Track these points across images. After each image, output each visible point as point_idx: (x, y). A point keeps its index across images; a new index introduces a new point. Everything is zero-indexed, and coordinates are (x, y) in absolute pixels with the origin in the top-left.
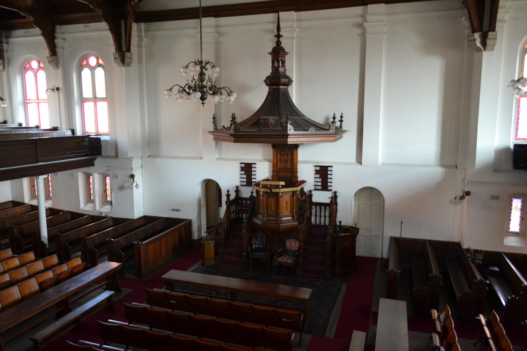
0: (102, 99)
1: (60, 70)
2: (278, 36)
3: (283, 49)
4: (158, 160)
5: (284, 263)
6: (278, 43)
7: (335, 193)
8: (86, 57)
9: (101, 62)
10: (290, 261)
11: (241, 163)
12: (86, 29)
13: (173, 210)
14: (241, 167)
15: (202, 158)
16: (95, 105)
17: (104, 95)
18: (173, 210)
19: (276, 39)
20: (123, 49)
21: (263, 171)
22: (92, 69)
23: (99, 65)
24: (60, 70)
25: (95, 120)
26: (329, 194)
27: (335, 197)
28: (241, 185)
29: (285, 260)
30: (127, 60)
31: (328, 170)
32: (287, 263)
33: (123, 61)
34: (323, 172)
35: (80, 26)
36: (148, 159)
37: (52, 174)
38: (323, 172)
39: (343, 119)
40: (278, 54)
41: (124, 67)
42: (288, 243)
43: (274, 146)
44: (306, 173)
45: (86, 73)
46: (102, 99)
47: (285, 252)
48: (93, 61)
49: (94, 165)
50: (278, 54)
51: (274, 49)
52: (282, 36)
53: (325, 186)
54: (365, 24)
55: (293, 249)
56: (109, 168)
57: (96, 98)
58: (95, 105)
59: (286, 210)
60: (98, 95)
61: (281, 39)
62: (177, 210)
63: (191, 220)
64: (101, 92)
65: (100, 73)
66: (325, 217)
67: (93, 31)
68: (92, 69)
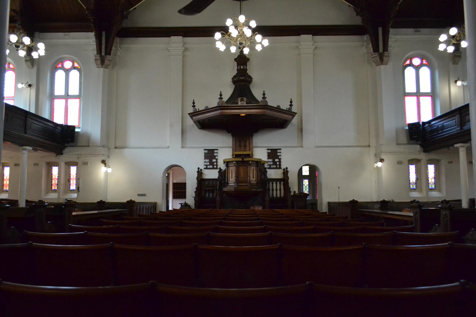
0: (74, 97)
1: (35, 70)
4: (126, 150)
8: (62, 61)
9: (76, 65)
11: (205, 150)
13: (139, 195)
14: (205, 153)
16: (67, 102)
17: (77, 93)
18: (139, 195)
20: (105, 53)
22: (67, 71)
23: (74, 68)
24: (35, 70)
25: (68, 113)
27: (286, 172)
28: (205, 168)
30: (106, 62)
31: (277, 152)
33: (103, 62)
34: (274, 154)
35: (61, 34)
36: (115, 149)
38: (274, 154)
41: (102, 69)
45: (60, 75)
46: (74, 97)
48: (68, 64)
49: (62, 154)
54: (300, 47)
56: (79, 156)
57: (68, 95)
58: (67, 102)
59: (253, 178)
60: (71, 93)
63: (156, 203)
64: (74, 89)
65: (75, 75)
66: (276, 190)
67: (73, 38)
68: (67, 71)
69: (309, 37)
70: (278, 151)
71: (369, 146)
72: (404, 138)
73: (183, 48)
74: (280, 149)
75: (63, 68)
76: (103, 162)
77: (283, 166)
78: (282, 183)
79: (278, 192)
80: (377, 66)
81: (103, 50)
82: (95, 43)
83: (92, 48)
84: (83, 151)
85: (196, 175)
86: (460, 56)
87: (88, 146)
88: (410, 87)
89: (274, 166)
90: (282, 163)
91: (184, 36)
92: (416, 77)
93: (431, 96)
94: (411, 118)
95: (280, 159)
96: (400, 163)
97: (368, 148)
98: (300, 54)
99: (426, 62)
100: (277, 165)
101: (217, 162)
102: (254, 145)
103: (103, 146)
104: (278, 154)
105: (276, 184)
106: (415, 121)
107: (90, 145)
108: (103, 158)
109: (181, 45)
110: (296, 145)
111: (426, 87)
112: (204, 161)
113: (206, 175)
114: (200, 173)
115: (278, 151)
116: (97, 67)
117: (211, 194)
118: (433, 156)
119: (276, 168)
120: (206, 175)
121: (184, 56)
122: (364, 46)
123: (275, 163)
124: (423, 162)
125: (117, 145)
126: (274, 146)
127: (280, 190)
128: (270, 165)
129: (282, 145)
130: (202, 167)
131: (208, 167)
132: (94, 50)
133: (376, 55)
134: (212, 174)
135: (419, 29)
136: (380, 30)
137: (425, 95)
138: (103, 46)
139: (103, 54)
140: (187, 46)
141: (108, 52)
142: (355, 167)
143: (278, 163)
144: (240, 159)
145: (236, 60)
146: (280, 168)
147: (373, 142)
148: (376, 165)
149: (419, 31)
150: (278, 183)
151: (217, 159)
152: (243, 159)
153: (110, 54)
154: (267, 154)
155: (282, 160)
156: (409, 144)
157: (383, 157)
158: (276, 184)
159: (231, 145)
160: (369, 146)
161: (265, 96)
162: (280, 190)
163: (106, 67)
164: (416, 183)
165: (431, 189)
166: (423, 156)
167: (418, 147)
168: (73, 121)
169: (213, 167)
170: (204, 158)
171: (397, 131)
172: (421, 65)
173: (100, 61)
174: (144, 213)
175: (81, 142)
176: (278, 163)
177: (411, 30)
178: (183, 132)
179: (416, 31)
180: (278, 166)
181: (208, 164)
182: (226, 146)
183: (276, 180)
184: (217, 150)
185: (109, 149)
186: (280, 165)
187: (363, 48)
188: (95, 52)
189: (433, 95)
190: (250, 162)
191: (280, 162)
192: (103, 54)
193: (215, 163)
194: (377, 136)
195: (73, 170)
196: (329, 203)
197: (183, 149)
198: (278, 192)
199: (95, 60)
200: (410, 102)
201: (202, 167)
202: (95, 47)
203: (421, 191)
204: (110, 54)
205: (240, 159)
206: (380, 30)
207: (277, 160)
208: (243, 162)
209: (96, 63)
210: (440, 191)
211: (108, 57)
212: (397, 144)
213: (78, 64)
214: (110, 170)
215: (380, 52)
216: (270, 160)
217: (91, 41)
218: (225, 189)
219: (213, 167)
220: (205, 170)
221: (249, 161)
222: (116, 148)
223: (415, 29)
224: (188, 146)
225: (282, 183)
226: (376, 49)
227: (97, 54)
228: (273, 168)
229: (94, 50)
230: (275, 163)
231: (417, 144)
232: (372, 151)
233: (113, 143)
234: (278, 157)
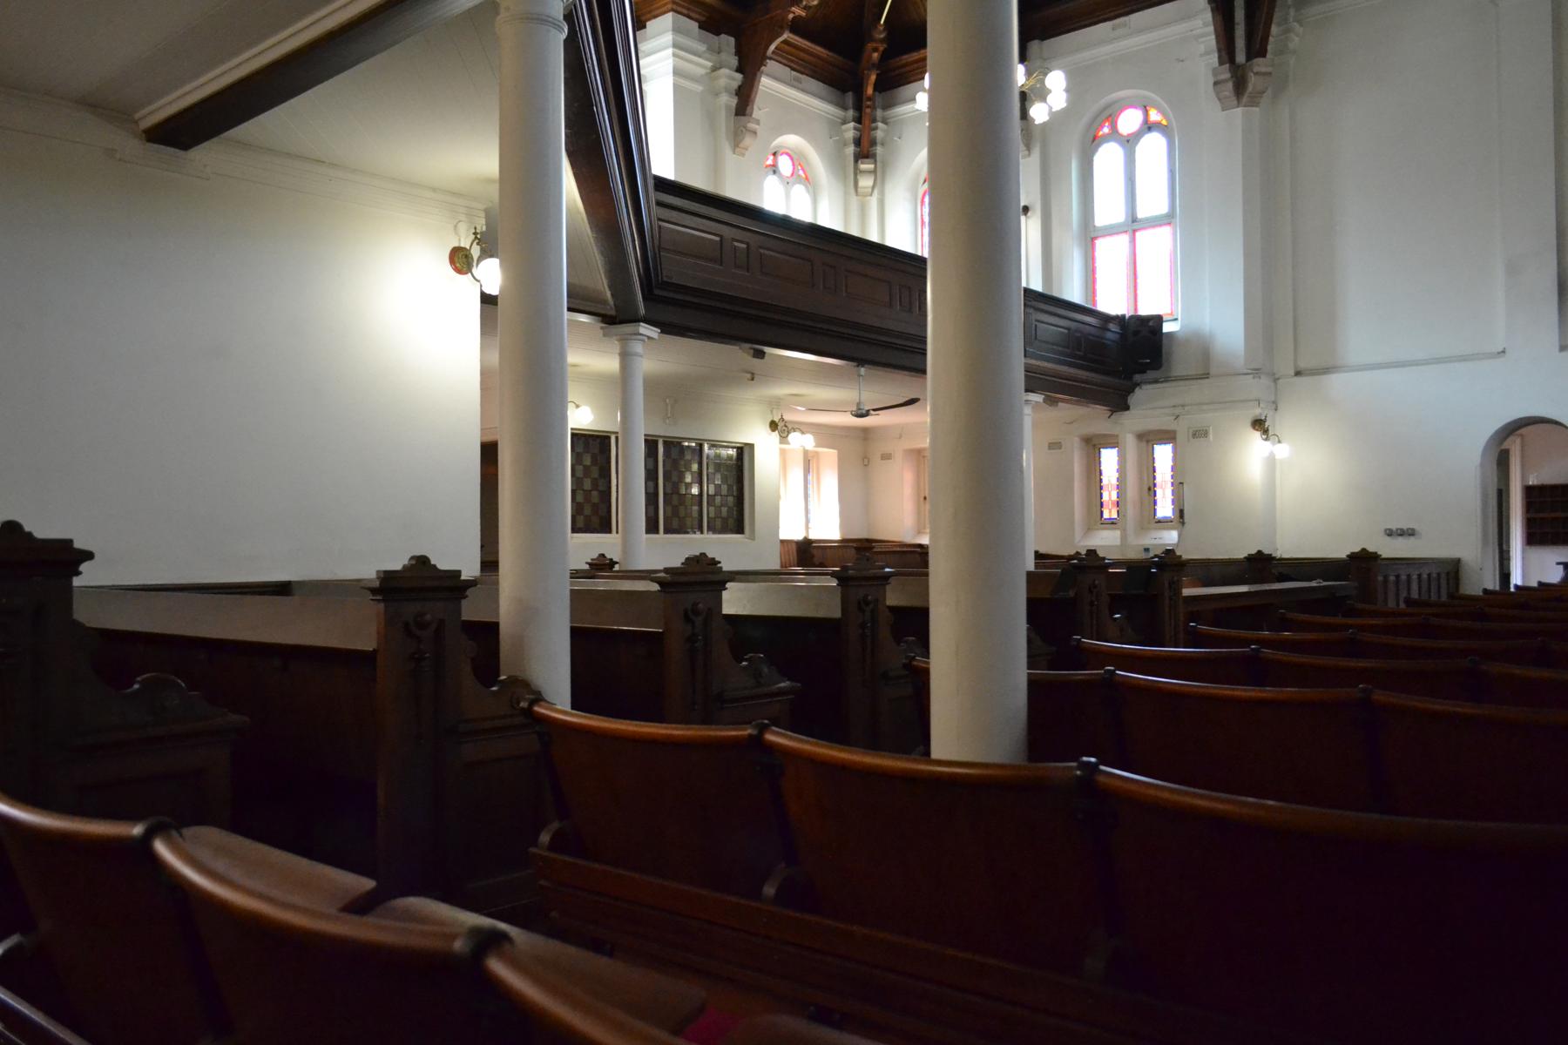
4: (1335, 381)
8: (1110, 115)
9: (1154, 116)
12: (1119, 32)
13: (1390, 533)
16: (1133, 241)
18: (1390, 533)
22: (1130, 142)
23: (1149, 127)
25: (1136, 275)
30: (1253, 82)
33: (1240, 86)
41: (1239, 110)
45: (1108, 158)
48: (1130, 120)
49: (1127, 408)
56: (1177, 411)
57: (1134, 220)
62: (1402, 533)
63: (1459, 561)
64: (1154, 197)
65: (1153, 148)
67: (1140, 31)
75: (1115, 134)
76: (1259, 424)
81: (1240, 43)
82: (1211, 28)
83: (1202, 48)
84: (1192, 393)
87: (1206, 376)
103: (1256, 372)
107: (1213, 371)
108: (1257, 412)
125: (1302, 365)
139: (1241, 57)
141: (1257, 48)
163: (1253, 103)
168: (1154, 299)
173: (1230, 85)
174: (1444, 598)
175: (1180, 363)
185: (1276, 380)
188: (1214, 59)
192: (1241, 57)
195: (1163, 455)
199: (1216, 84)
202: (1211, 41)
209: (1217, 94)
211: (1260, 64)
213: (1161, 111)
214: (1282, 451)
217: (1198, 22)
222: (1298, 373)
227: (1221, 63)
229: (1207, 53)
233: (1290, 356)
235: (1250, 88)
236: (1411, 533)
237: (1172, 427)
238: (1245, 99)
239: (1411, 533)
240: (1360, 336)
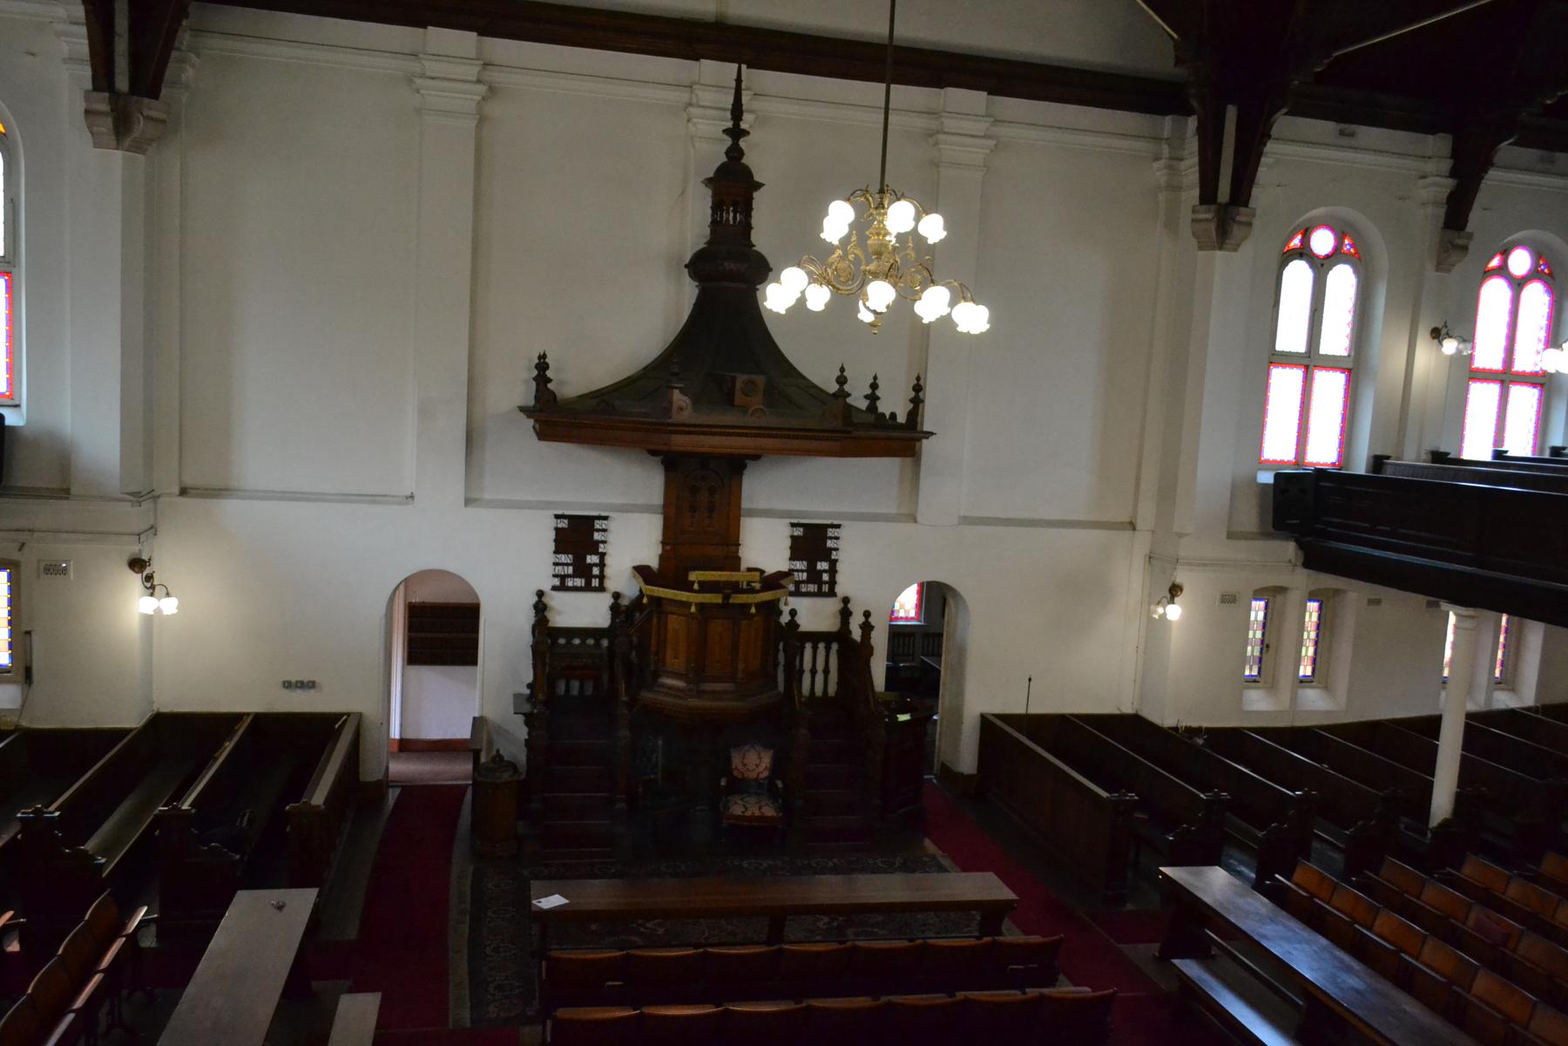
2: (736, 133)
3: (747, 173)
5: (753, 818)
6: (735, 153)
7: (846, 600)
10: (769, 811)
11: (557, 517)
13: (288, 685)
15: (412, 497)
18: (288, 685)
19: (728, 142)
21: (632, 544)
26: (831, 606)
29: (753, 811)
30: (140, 127)
31: (826, 538)
32: (763, 818)
34: (813, 544)
37: (1463, 611)
38: (813, 544)
39: (878, 393)
40: (733, 186)
41: (119, 154)
42: (736, 761)
43: (673, 464)
44: (764, 547)
47: (740, 786)
50: (733, 186)
51: (722, 171)
52: (745, 133)
53: (823, 584)
55: (753, 775)
56: (23, 537)
61: (743, 143)
66: (813, 672)
69: (976, 99)
70: (831, 532)
71: (1132, 526)
72: (1249, 518)
73: (482, 88)
74: (838, 526)
76: (137, 564)
77: (841, 590)
78: (835, 647)
79: (820, 678)
80: (1200, 248)
82: (84, 30)
84: (45, 514)
85: (526, 619)
86: (1465, 248)
87: (64, 493)
88: (1291, 337)
89: (812, 588)
90: (839, 578)
91: (484, 32)
92: (1317, 302)
93: (1348, 372)
94: (1278, 446)
95: (833, 563)
96: (1229, 599)
97: (1128, 533)
98: (935, 164)
99: (1352, 246)
100: (820, 583)
101: (602, 565)
102: (745, 504)
103: (138, 497)
104: (830, 544)
105: (815, 649)
106: (1289, 455)
107: (73, 491)
108: (133, 549)
109: (472, 71)
110: (893, 511)
111: (1336, 340)
112: (552, 558)
113: (560, 613)
114: (541, 608)
115: (831, 532)
116: (96, 145)
117: (575, 685)
118: (1329, 581)
119: (820, 594)
120: (560, 613)
121: (482, 120)
122: (1162, 163)
123: (814, 576)
124: (1294, 597)
125: (189, 481)
126: (817, 509)
127: (826, 672)
128: (798, 584)
129: (845, 508)
130: (547, 583)
131: (570, 583)
132: (72, 59)
133: (1207, 214)
134: (584, 611)
135: (1353, 127)
136: (1231, 113)
137: (1331, 364)
138: (121, 46)
139: (122, 83)
140: (495, 76)
141: (148, 81)
142: (1081, 594)
143: (826, 577)
144: (716, 599)
145: (709, 182)
146: (832, 593)
147: (1147, 515)
148: (1160, 610)
149: (1352, 135)
150: (821, 646)
151: (602, 556)
152: (726, 597)
153: (155, 94)
154: (788, 542)
155: (839, 567)
156: (1264, 535)
157: (1181, 577)
158: (815, 649)
159: (657, 498)
160: (1132, 526)
161: (846, 387)
162: (826, 672)
163: (138, 148)
164: (1260, 660)
165: (1304, 681)
166: (1301, 579)
167: (1291, 547)
169: (588, 583)
170: (552, 547)
171: (1234, 487)
172: (1335, 257)
175: (24, 474)
176: (826, 577)
177: (1325, 128)
178: (472, 440)
179: (1342, 133)
180: (826, 588)
181: (570, 570)
182: (640, 501)
183: (815, 637)
184: (606, 518)
186: (832, 583)
187: (1156, 165)
189: (1354, 368)
190: (753, 610)
191: (833, 571)
192: (122, 83)
193: (596, 571)
194: (1167, 494)
196: (983, 718)
197: (471, 510)
198: (820, 678)
199: (87, 112)
200: (1284, 384)
201: (546, 588)
202: (80, 43)
203: (1272, 687)
204: (155, 94)
205: (716, 599)
206: (1231, 113)
207: (822, 566)
208: (725, 605)
209: (90, 127)
210: (1327, 688)
211: (151, 108)
212: (1231, 535)
214: (169, 606)
215: (1226, 203)
216: (800, 565)
218: (647, 695)
219: (588, 583)
220: (554, 593)
221: (749, 606)
222: (184, 492)
223: (1342, 126)
224: (487, 496)
225: (835, 647)
226: (1208, 195)
227: (97, 87)
228: (808, 594)
229: (79, 61)
230: (814, 576)
231: (1287, 539)
232: (1142, 543)
233: (175, 473)
234: (826, 554)
235: (136, 134)
236: (312, 685)
237: (16, 556)
238: (127, 143)
239: (312, 685)
240: (258, 458)
